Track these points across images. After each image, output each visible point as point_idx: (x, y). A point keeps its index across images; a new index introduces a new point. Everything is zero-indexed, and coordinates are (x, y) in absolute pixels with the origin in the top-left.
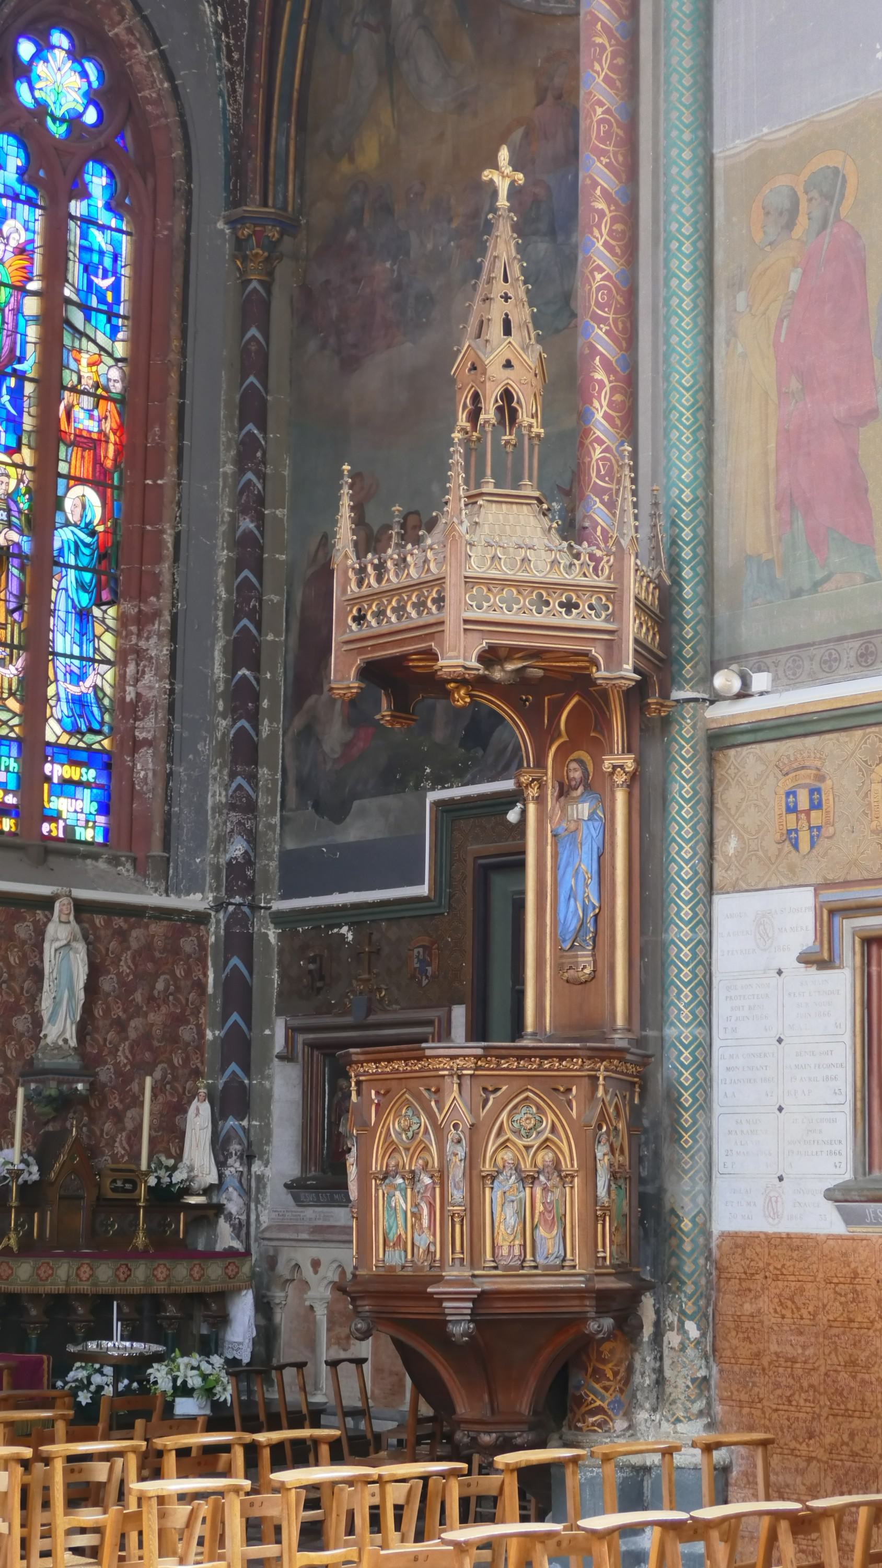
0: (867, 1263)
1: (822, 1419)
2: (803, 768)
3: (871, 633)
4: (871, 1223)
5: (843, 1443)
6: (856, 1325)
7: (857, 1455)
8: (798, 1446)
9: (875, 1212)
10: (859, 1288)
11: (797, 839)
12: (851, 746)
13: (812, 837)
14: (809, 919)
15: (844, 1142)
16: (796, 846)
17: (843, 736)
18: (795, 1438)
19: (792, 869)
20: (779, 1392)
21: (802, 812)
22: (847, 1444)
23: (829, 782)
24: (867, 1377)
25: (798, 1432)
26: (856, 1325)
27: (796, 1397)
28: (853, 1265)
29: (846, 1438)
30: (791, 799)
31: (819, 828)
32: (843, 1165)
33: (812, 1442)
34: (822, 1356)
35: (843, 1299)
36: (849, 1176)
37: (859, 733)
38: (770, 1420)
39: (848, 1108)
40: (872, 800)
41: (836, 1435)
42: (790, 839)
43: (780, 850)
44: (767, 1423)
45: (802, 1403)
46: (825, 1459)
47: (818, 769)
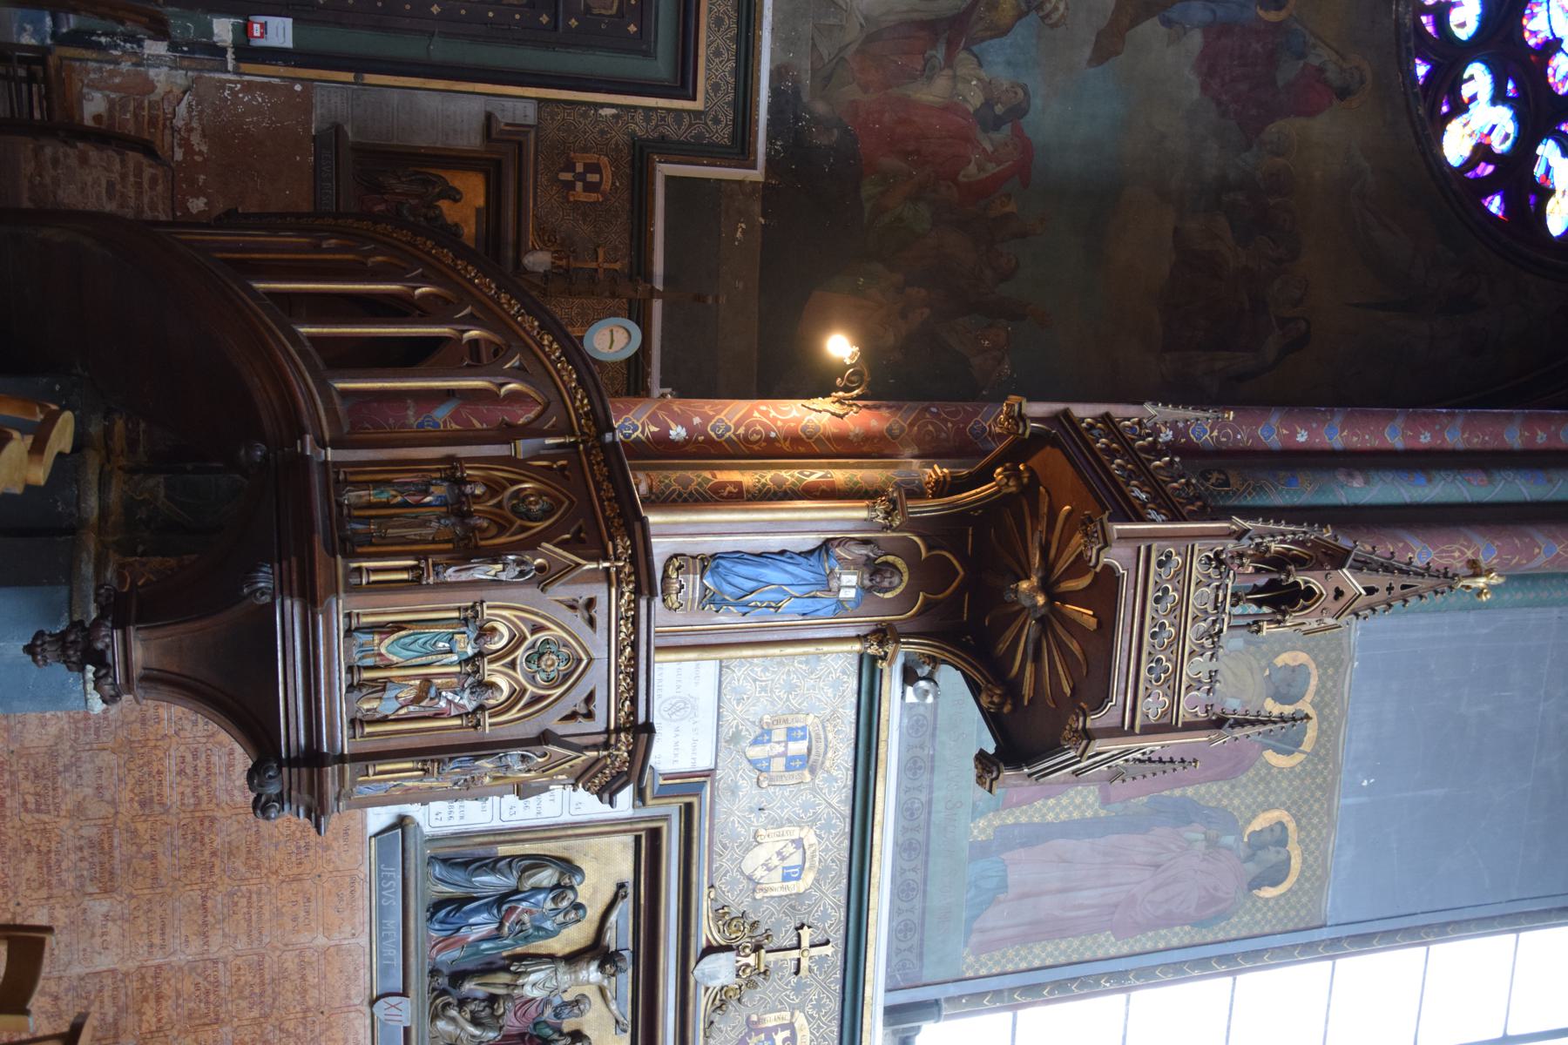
0: (338, 862)
1: (164, 817)
2: (826, 746)
3: (930, 813)
4: (380, 871)
5: (140, 846)
6: (272, 853)
7: (129, 865)
8: (129, 787)
9: (391, 878)
10: (311, 853)
11: (763, 743)
12: (834, 802)
13: (760, 761)
14: (684, 765)
15: (463, 822)
16: (755, 742)
17: (847, 792)
18: (140, 782)
19: (736, 738)
20: (189, 758)
21: (786, 746)
22: (139, 851)
23: (807, 776)
24: (217, 870)
25: (145, 786)
26: (272, 853)
27: (185, 782)
28: (335, 845)
29: (147, 849)
30: (800, 733)
31: (768, 769)
32: (438, 823)
33: (136, 805)
34: (233, 811)
35: (298, 834)
36: (427, 830)
37: (847, 811)
38: (155, 747)
39: (496, 824)
40: (785, 829)
41: (147, 837)
42: (762, 735)
43: (754, 723)
44: (152, 744)
45: (181, 789)
46: (119, 824)
47: (823, 763)
